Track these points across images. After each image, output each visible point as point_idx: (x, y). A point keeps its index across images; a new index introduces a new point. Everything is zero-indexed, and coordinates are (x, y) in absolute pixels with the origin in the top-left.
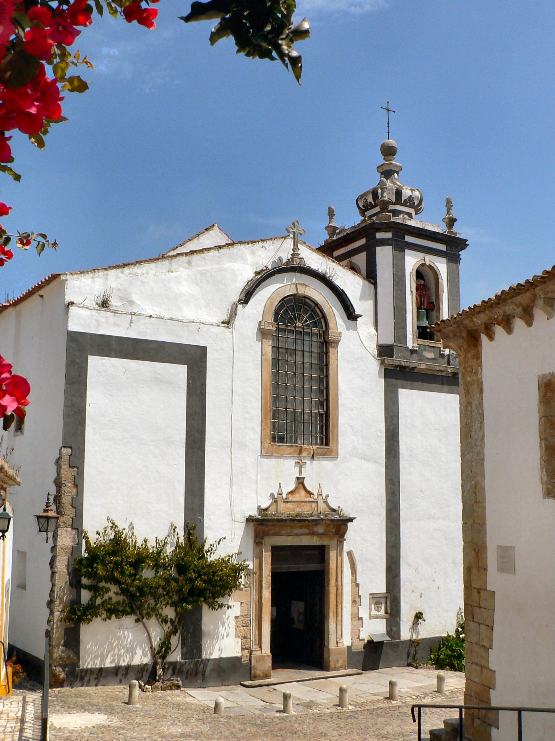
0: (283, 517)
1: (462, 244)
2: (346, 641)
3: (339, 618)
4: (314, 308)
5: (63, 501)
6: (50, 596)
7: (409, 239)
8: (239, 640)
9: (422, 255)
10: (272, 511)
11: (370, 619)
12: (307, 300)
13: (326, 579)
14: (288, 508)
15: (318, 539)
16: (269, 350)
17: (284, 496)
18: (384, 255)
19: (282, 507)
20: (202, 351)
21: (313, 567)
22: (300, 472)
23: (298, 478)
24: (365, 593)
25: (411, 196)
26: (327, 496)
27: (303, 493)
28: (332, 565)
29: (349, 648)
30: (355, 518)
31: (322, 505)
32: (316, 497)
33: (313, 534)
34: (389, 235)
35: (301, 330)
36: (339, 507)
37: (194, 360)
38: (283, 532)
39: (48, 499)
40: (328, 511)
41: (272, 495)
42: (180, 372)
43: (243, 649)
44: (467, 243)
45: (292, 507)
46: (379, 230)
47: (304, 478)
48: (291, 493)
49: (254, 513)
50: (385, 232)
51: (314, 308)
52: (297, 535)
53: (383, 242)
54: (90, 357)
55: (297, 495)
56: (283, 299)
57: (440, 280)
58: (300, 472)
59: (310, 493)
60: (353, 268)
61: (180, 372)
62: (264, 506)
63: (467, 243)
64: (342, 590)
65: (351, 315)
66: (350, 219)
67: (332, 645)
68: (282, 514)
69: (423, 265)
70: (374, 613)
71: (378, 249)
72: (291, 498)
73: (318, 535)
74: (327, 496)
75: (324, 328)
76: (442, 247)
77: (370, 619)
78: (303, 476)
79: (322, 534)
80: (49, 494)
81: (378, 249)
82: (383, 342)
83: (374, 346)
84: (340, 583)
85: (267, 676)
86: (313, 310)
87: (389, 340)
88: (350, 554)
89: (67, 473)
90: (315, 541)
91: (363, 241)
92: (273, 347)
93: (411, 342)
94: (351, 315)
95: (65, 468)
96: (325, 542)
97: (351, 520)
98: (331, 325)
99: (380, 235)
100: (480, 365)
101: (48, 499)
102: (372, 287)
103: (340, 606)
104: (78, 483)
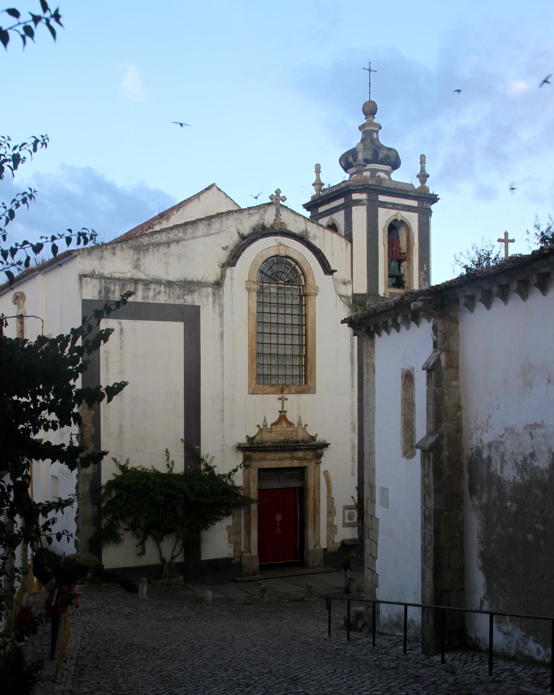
0: (267, 444)
1: (434, 199)
2: (324, 544)
3: (317, 526)
4: (294, 266)
6: (77, 513)
7: (381, 198)
8: (232, 545)
9: (393, 212)
10: (258, 438)
11: (344, 526)
12: (288, 260)
13: (306, 494)
14: (272, 437)
15: (298, 462)
17: (269, 427)
18: (359, 215)
19: (266, 437)
21: (294, 484)
23: (280, 412)
24: (339, 506)
25: (387, 155)
26: (306, 425)
27: (284, 424)
28: (311, 482)
29: (325, 550)
30: (329, 444)
32: (296, 426)
33: (293, 458)
34: (364, 196)
35: (283, 286)
36: (317, 435)
38: (268, 457)
39: (71, 438)
40: (306, 438)
41: (258, 426)
42: (177, 329)
43: (234, 552)
44: (438, 197)
45: (275, 436)
46: (355, 191)
47: (285, 412)
48: (275, 424)
49: (243, 440)
50: (361, 193)
51: (294, 266)
52: (280, 459)
53: (358, 202)
55: (279, 426)
56: (266, 261)
57: (411, 233)
59: (290, 424)
60: (333, 227)
61: (177, 329)
62: (251, 436)
63: (438, 197)
64: (319, 503)
65: (328, 270)
66: (336, 176)
67: (311, 547)
68: (267, 442)
69: (396, 220)
70: (347, 521)
71: (354, 208)
72: (274, 428)
73: (299, 459)
74: (306, 425)
75: (303, 283)
76: (414, 203)
77: (344, 526)
78: (285, 409)
79: (302, 457)
80: (71, 434)
81: (354, 208)
84: (317, 498)
85: (254, 573)
86: (294, 268)
88: (326, 473)
90: (296, 464)
91: (341, 201)
92: (257, 302)
93: (382, 290)
94: (328, 270)
96: (304, 464)
97: (326, 445)
98: (310, 280)
99: (355, 196)
100: (374, 353)
101: (71, 438)
103: (317, 516)
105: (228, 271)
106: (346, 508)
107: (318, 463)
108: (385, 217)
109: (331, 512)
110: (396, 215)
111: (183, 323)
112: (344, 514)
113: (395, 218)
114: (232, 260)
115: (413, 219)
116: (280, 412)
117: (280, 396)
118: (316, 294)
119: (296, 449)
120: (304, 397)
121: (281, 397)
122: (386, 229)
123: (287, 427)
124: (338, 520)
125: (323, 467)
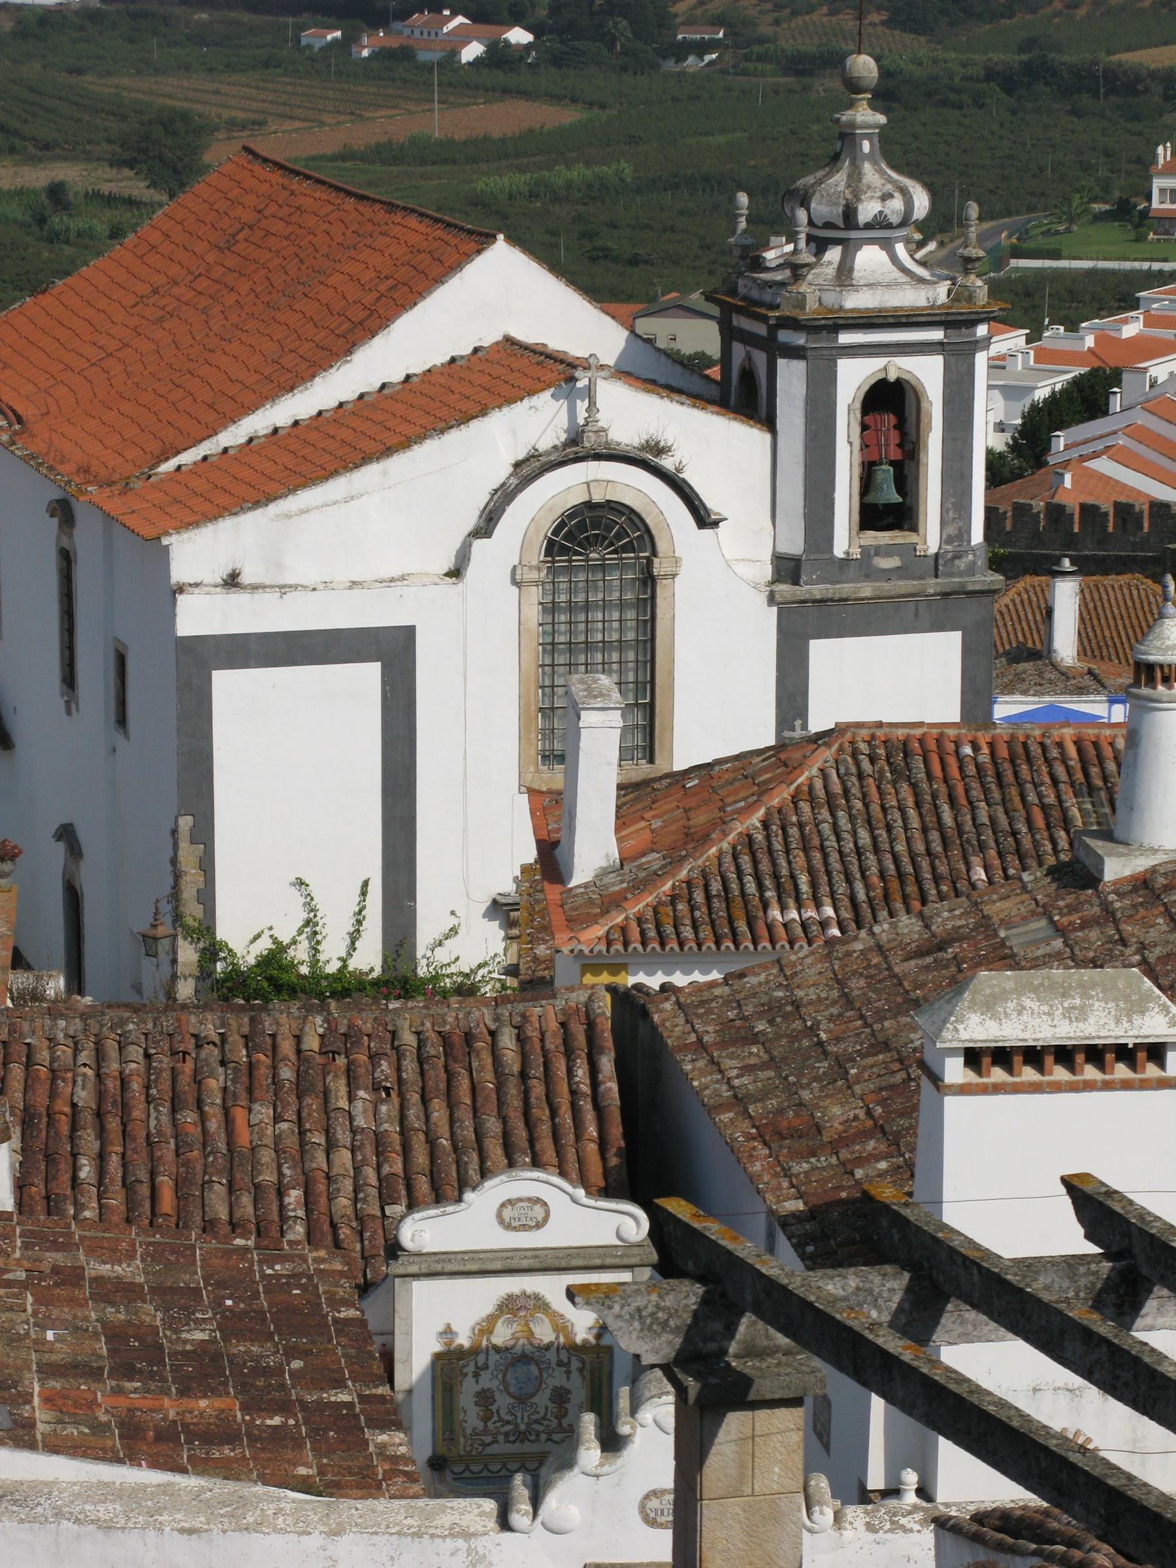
5: (185, 895)
7: (845, 338)
16: (534, 614)
18: (791, 379)
20: (408, 634)
37: (393, 651)
54: (214, 673)
57: (924, 405)
65: (703, 518)
76: (937, 335)
82: (785, 548)
83: (767, 556)
87: (794, 545)
89: (188, 854)
94: (703, 518)
95: (184, 845)
98: (661, 546)
102: (767, 437)
104: (207, 865)
105: (478, 545)
108: (853, 377)
110: (885, 368)
111: (377, 666)
113: (881, 376)
114: (487, 524)
115: (928, 373)
118: (674, 576)
122: (858, 405)
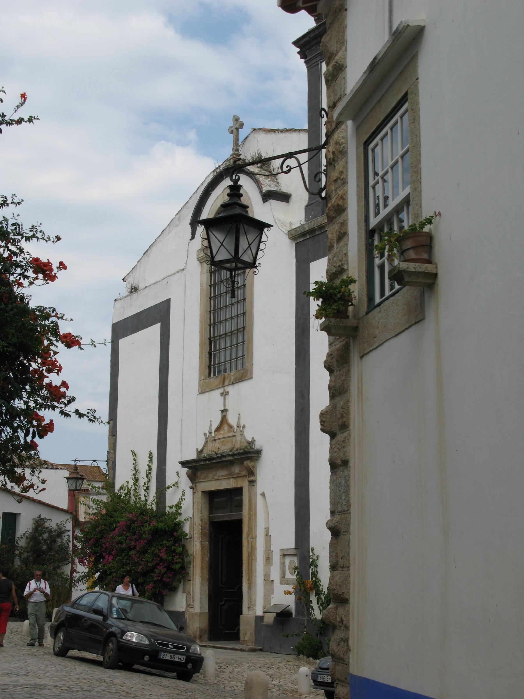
22: (224, 405)
23: (222, 411)
29: (259, 619)
31: (238, 438)
48: (218, 429)
55: (222, 432)
58: (224, 405)
59: (230, 427)
74: (244, 427)
78: (227, 408)
106: (285, 555)
107: (252, 483)
109: (268, 559)
112: (283, 564)
116: (222, 411)
117: (221, 390)
119: (231, 463)
120: (244, 386)
121: (222, 392)
123: (228, 432)
124: (275, 575)
125: (260, 487)
